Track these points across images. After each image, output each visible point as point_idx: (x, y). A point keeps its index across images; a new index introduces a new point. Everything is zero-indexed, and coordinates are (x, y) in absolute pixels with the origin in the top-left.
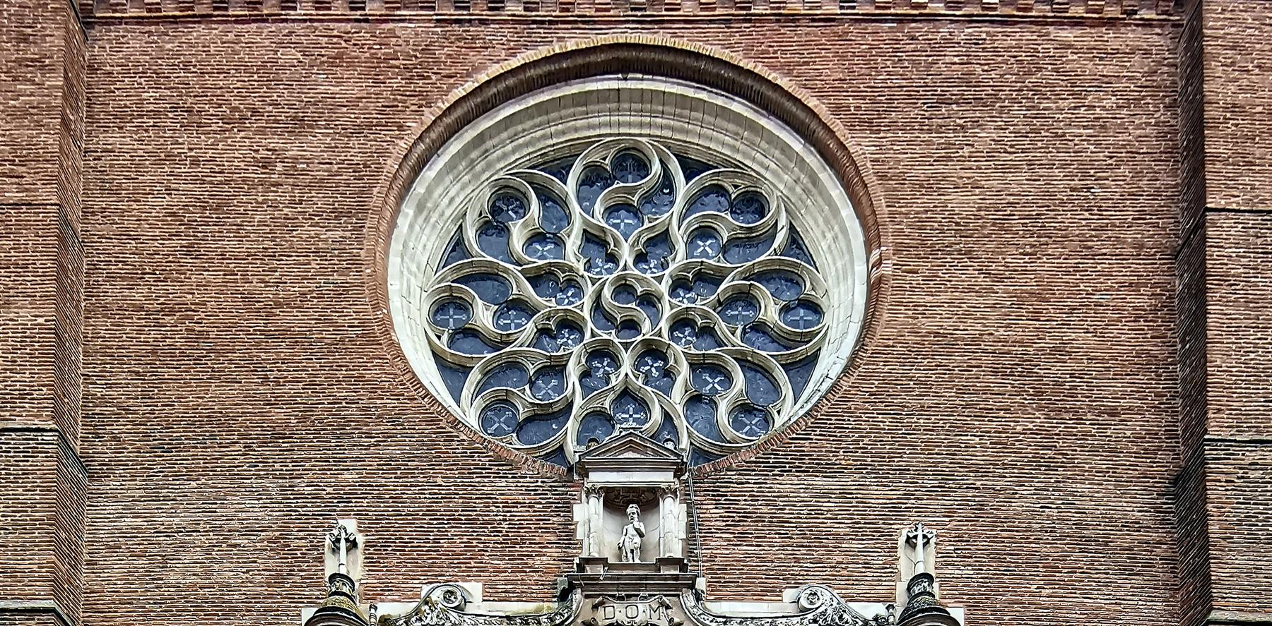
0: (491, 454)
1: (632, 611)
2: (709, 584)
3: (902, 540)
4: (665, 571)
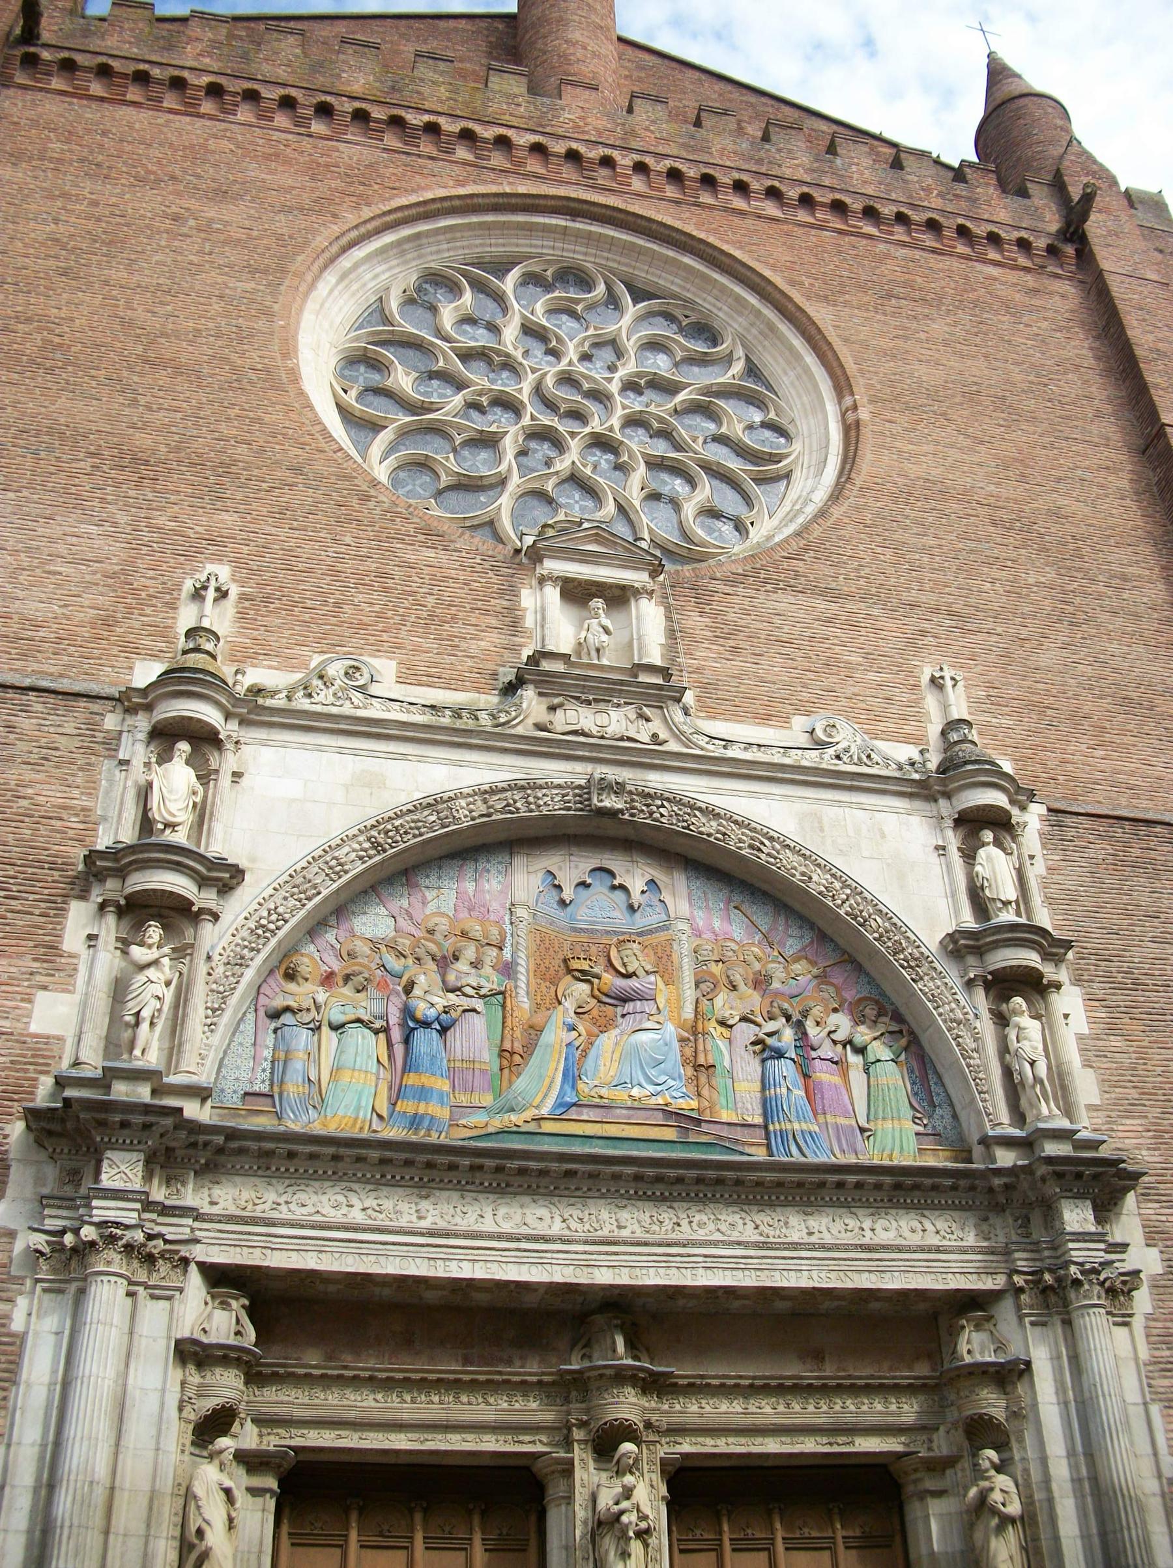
0: (418, 520)
1: (602, 719)
2: (698, 699)
3: (925, 679)
4: (644, 678)
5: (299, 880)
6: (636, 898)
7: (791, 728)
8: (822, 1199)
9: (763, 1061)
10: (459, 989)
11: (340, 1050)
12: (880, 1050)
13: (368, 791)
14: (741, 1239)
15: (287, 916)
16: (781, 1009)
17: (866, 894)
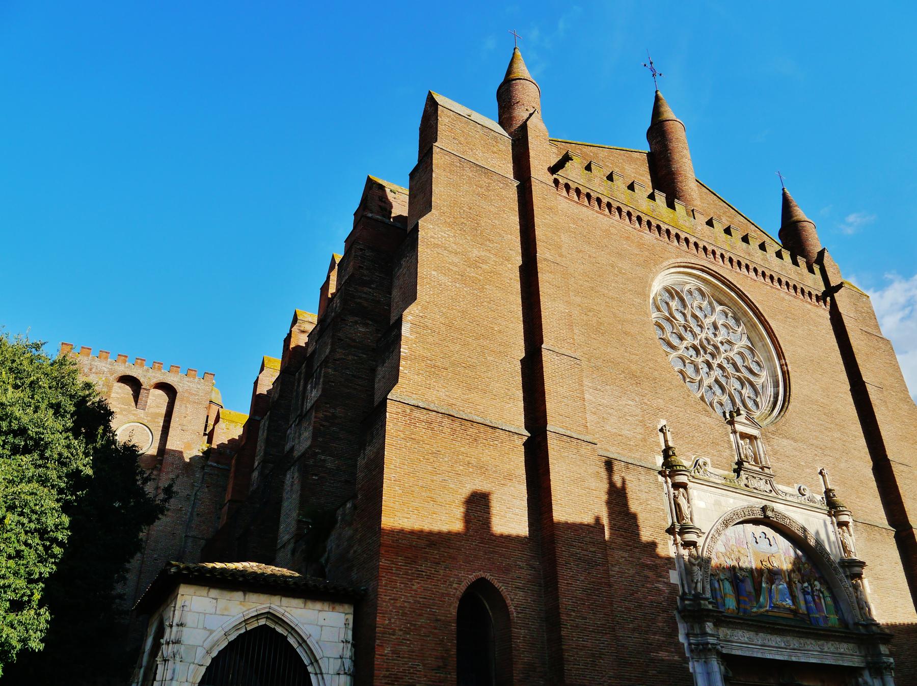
7: (794, 488)
9: (804, 595)
12: (826, 593)
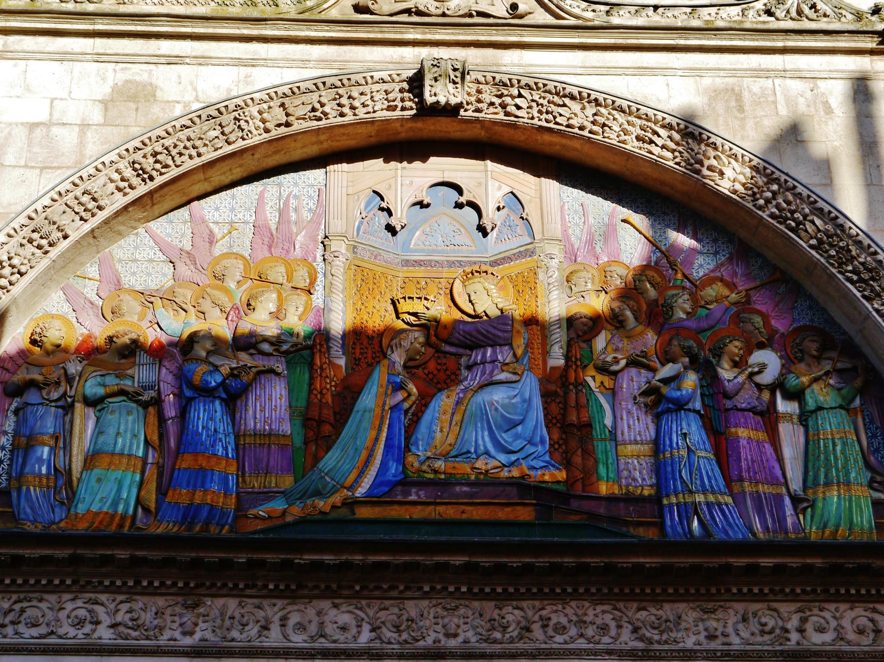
5: (39, 220)
6: (490, 215)
8: (728, 590)
10: (254, 346)
11: (99, 431)
13: (133, 106)
14: (612, 647)
15: (23, 269)
16: (683, 348)
17: (800, 189)
